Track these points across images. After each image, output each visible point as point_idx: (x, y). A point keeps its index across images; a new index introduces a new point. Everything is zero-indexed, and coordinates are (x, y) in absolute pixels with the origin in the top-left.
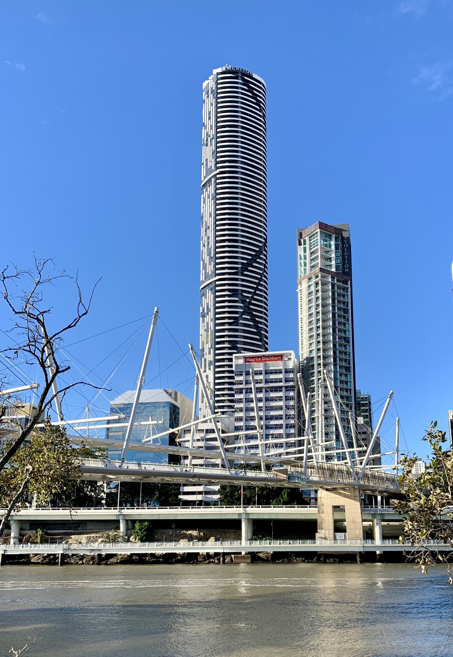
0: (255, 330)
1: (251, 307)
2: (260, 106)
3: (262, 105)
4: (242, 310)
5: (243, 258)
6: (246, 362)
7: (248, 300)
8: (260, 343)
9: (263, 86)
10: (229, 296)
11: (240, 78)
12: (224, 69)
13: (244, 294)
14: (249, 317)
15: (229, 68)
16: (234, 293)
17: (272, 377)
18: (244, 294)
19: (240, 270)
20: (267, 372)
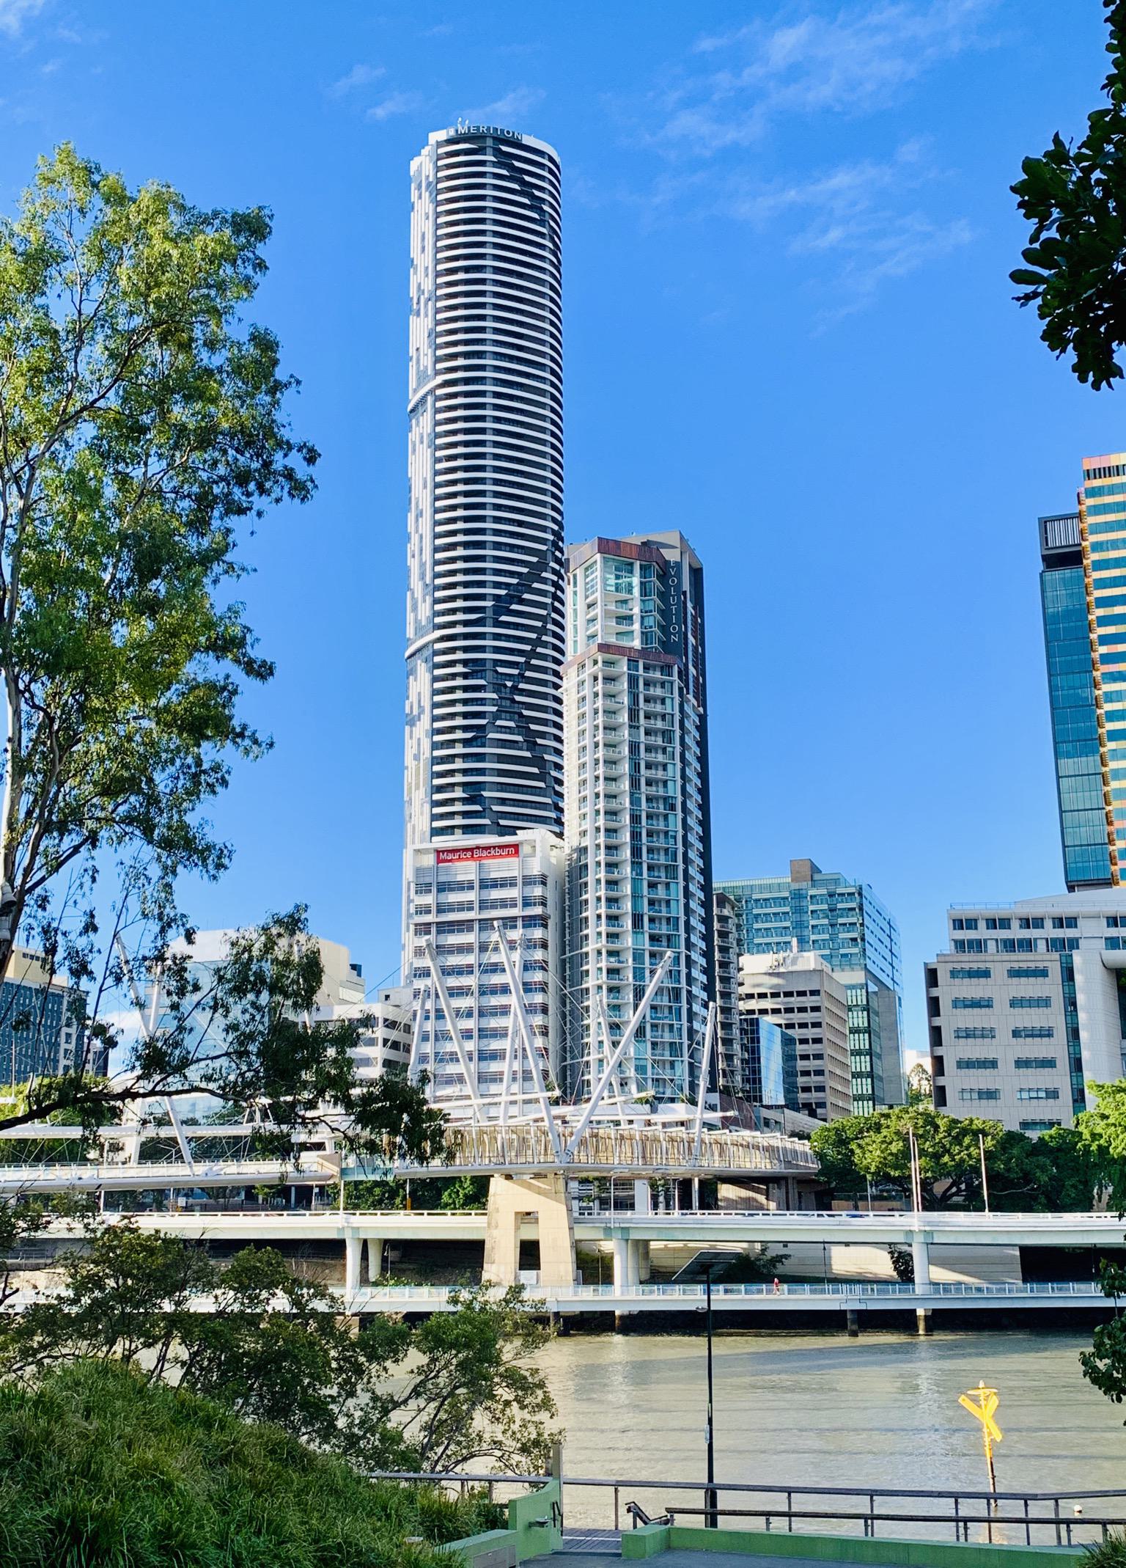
0: (528, 754)
1: (518, 698)
2: (542, 212)
3: (546, 208)
4: (494, 709)
5: (497, 585)
6: (439, 861)
7: (509, 684)
8: (542, 785)
9: (551, 160)
10: (465, 676)
12: (452, 133)
13: (500, 670)
14: (512, 724)
16: (475, 668)
17: (496, 894)
18: (500, 670)
19: (489, 613)
20: (486, 884)
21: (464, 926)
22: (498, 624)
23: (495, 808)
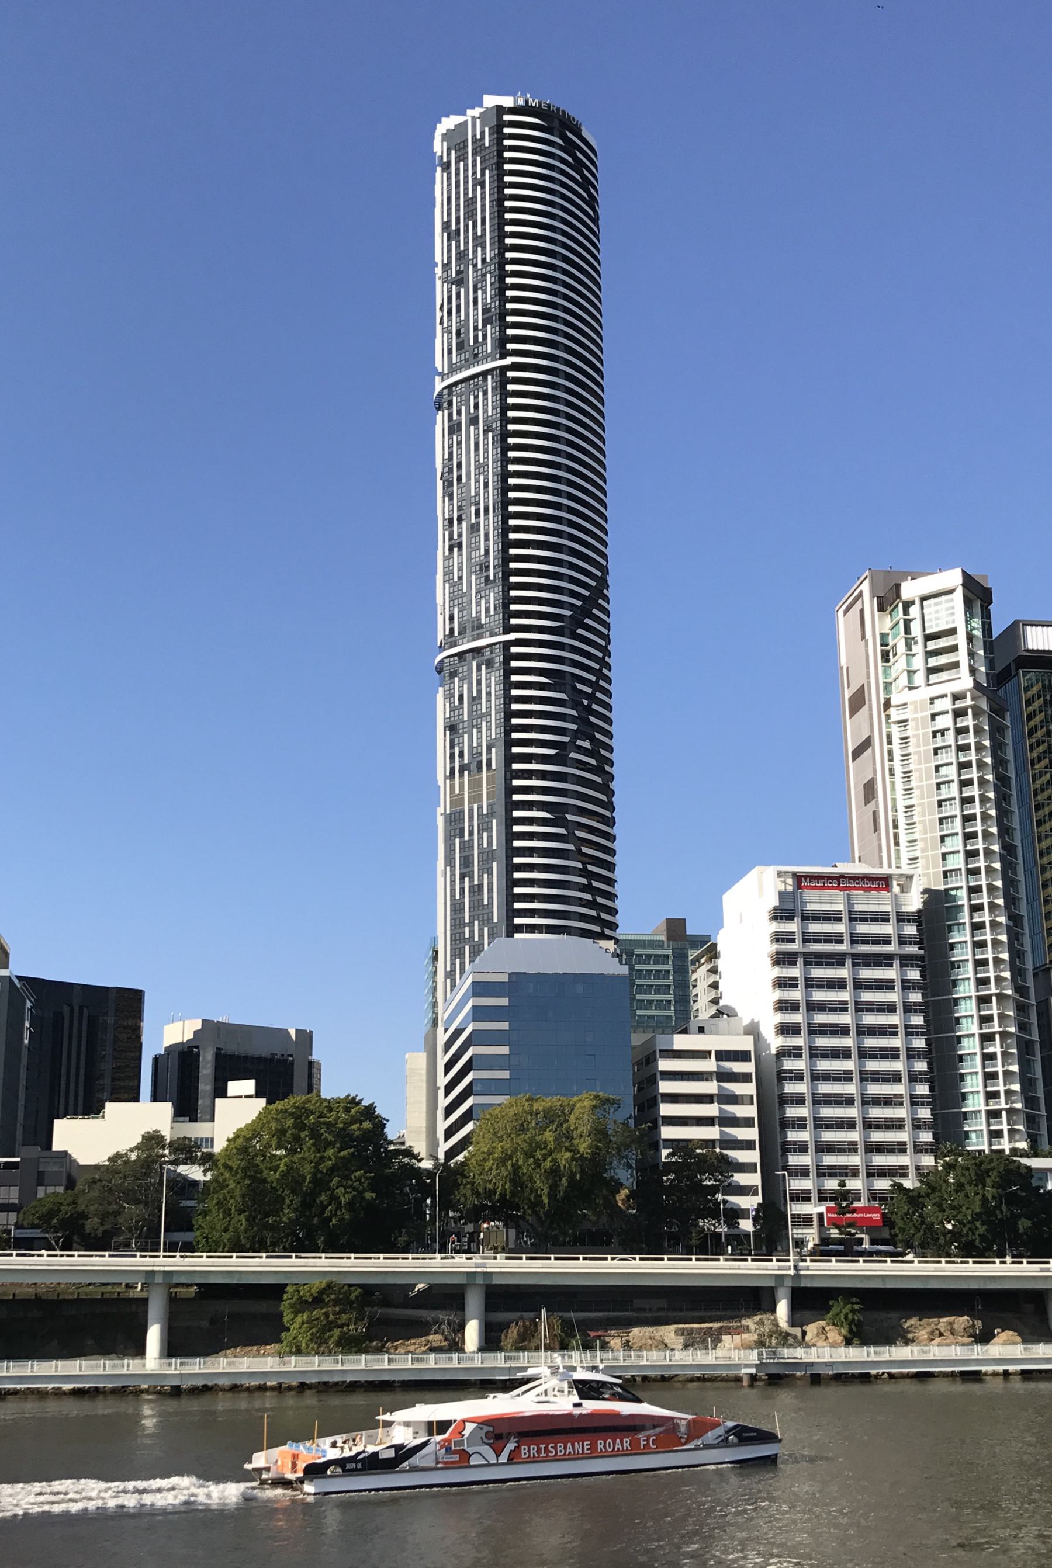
1: (592, 719)
4: (575, 727)
5: (574, 594)
6: (799, 886)
7: (586, 702)
11: (556, 132)
12: (521, 102)
13: (579, 686)
15: (534, 103)
17: (862, 928)
18: (579, 686)
20: (855, 918)
21: (838, 960)
22: (575, 636)
23: (578, 834)
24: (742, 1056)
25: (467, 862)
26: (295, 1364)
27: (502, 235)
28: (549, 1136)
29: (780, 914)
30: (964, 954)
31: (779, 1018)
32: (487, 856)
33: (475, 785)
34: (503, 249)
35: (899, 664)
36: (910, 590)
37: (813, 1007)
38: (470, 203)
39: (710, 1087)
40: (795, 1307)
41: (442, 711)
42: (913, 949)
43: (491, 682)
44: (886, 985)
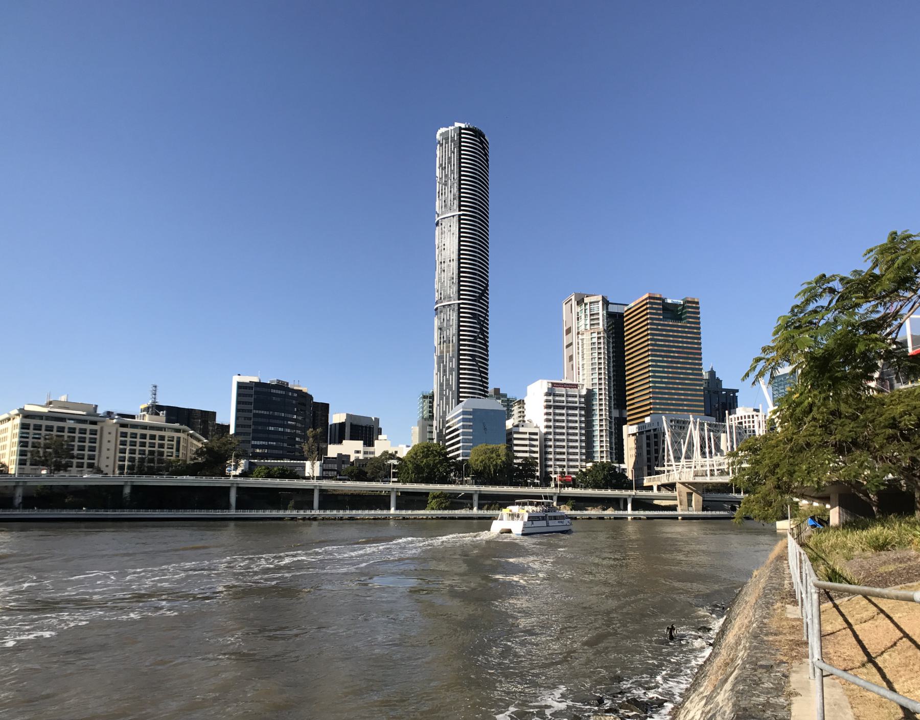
17: (570, 399)
20: (568, 396)
21: (563, 408)
24: (536, 434)
25: (445, 371)
26: (433, 512)
27: (460, 171)
28: (494, 455)
29: (548, 394)
30: (597, 408)
31: (546, 423)
32: (451, 370)
33: (448, 347)
34: (460, 175)
35: (582, 322)
36: (587, 300)
37: (555, 421)
38: (450, 158)
39: (527, 442)
40: (558, 501)
41: (436, 323)
42: (583, 405)
43: (454, 316)
44: (575, 415)
